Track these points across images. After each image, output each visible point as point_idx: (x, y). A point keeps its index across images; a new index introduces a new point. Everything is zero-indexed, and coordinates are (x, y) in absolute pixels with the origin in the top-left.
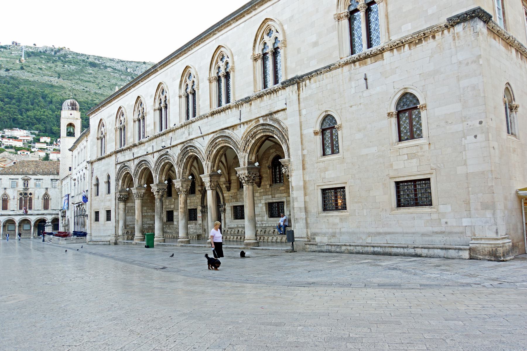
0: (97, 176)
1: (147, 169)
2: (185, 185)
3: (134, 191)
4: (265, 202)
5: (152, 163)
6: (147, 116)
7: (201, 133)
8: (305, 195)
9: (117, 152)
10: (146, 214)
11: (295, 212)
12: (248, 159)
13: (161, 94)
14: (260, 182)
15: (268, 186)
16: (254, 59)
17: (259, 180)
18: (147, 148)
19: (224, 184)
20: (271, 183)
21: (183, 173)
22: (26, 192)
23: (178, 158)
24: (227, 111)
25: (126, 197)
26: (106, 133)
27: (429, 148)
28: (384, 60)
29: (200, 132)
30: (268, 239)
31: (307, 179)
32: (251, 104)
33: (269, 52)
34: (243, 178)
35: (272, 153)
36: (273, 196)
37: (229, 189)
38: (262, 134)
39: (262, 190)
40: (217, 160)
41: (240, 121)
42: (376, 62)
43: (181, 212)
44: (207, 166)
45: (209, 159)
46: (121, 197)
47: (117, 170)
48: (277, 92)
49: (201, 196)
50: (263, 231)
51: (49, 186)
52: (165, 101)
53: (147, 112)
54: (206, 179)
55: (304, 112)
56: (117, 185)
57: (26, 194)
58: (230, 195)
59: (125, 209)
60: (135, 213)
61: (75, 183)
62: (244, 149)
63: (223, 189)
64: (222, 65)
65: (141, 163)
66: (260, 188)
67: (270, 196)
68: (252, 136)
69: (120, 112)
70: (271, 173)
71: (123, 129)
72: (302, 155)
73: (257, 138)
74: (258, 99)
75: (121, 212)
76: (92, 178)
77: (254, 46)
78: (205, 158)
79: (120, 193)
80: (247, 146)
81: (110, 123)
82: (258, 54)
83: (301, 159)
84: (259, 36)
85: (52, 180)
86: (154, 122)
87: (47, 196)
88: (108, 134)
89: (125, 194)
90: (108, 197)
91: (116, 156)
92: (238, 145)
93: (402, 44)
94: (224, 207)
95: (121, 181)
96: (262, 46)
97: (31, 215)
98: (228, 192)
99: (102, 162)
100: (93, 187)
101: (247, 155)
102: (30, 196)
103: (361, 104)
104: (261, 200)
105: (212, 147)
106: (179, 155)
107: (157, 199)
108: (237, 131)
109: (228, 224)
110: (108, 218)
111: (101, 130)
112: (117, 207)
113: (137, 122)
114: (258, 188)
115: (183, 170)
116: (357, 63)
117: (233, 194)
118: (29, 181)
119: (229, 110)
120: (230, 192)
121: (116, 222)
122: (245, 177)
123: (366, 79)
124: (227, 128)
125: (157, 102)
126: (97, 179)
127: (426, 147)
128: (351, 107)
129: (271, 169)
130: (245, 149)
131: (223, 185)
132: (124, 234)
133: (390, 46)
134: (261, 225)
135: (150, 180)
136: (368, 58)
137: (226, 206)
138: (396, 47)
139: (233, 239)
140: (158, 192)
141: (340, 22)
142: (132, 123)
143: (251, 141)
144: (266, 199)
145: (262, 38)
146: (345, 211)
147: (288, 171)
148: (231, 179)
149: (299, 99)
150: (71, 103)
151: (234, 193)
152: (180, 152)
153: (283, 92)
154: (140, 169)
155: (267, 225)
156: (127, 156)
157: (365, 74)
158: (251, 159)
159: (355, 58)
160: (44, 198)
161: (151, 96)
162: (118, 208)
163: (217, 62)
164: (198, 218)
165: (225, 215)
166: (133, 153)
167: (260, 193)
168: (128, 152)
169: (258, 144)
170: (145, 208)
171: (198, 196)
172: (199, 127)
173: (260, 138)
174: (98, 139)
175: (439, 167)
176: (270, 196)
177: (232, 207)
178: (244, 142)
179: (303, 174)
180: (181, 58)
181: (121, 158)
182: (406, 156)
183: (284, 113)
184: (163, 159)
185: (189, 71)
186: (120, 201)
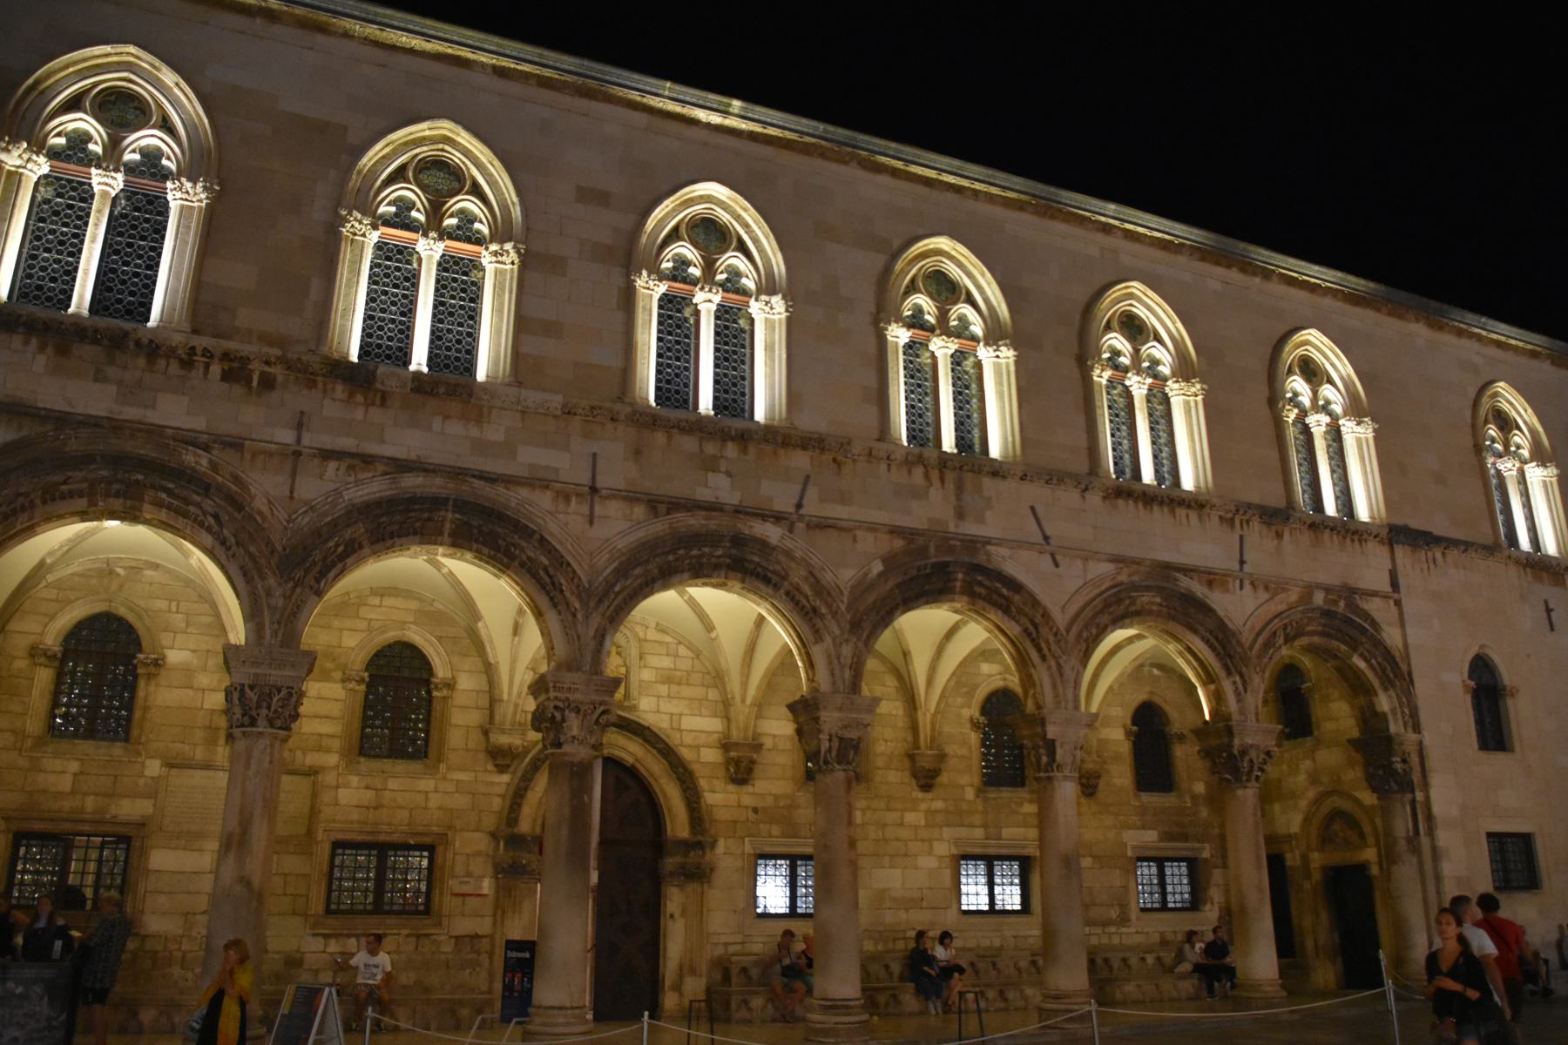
15: (970, 794)
39: (939, 805)
48: (1363, 543)
58: (747, 801)
66: (930, 795)
98: (731, 787)
104: (935, 844)
109: (723, 939)
114: (920, 795)
120: (749, 789)
151: (776, 797)
167: (929, 812)
172: (1033, 509)
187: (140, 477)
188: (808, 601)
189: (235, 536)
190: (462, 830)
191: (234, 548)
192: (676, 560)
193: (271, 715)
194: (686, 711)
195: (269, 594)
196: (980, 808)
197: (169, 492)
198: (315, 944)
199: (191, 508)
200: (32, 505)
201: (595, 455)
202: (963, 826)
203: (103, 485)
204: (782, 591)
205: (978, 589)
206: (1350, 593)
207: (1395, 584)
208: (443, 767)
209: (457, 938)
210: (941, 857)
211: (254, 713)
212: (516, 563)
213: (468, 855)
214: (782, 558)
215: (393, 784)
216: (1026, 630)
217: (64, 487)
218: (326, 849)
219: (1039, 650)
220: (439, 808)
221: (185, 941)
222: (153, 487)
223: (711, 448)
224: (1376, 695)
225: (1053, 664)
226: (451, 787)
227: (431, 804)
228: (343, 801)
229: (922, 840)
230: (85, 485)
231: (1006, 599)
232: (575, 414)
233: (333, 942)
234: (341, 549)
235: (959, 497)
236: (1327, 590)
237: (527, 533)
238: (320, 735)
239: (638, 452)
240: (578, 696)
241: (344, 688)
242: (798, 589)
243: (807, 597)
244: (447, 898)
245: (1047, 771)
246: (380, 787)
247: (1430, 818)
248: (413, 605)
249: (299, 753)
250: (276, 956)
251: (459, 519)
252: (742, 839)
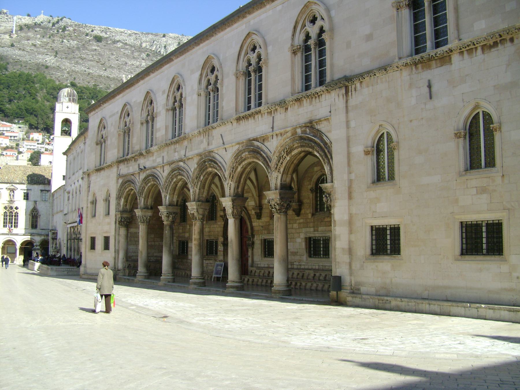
0: (94, 192)
1: (155, 186)
2: (201, 211)
3: (138, 212)
4: (305, 236)
5: (162, 179)
6: (158, 118)
7: (224, 143)
8: (351, 232)
9: (120, 162)
10: (153, 243)
11: (337, 254)
12: (281, 181)
13: (176, 90)
14: (300, 210)
15: (310, 216)
16: (293, 52)
17: (298, 207)
18: (156, 159)
19: (253, 209)
20: (314, 212)
21: (199, 194)
22: (11, 205)
23: (193, 173)
24: (256, 116)
25: (128, 221)
26: (107, 137)
27: (503, 181)
28: (451, 64)
29: (222, 142)
30: (305, 286)
31: (354, 211)
32: (287, 109)
33: (312, 45)
34: (274, 205)
35: (317, 171)
36: (316, 228)
37: (259, 216)
38: (300, 149)
39: (302, 221)
40: (242, 180)
41: (273, 131)
42: (442, 66)
43: (195, 244)
44: (229, 187)
45: (232, 178)
46: (123, 220)
47: (119, 185)
48: (320, 96)
49: (223, 223)
50: (301, 274)
51: (38, 199)
52: (181, 100)
53: (158, 111)
54: (227, 203)
55: (353, 124)
56: (118, 204)
57: (11, 208)
58: (261, 224)
59: (127, 236)
60: (138, 241)
61: (69, 197)
62: (276, 168)
63: (251, 216)
64: (253, 57)
65: (148, 179)
66: (299, 218)
67: (312, 229)
68: (286, 151)
69: (125, 112)
70: (314, 198)
71: (127, 132)
72: (348, 179)
73: (293, 153)
74: (296, 104)
75: (122, 240)
76: (88, 194)
77: (293, 35)
78: (226, 176)
79: (121, 215)
80: (280, 164)
81: (112, 124)
82: (297, 46)
83: (347, 185)
84: (300, 23)
85: (42, 191)
86: (166, 126)
87: (36, 212)
88: (109, 138)
89: (127, 217)
90: (107, 220)
91: (118, 167)
92: (269, 162)
93: (474, 47)
94: (253, 240)
95: (123, 200)
96: (302, 37)
97: (17, 235)
98: (258, 221)
99: (101, 173)
100: (89, 205)
101: (280, 176)
102: (16, 211)
103: (422, 119)
105: (237, 162)
106: (195, 169)
107: (166, 225)
108: (269, 143)
110: (107, 247)
111: (101, 133)
112: (117, 232)
113: (145, 125)
114: (297, 218)
115: (199, 190)
116: (419, 66)
117: (265, 223)
118: (15, 191)
119: (260, 116)
120: (261, 220)
121: (115, 252)
122: (276, 204)
123: (430, 86)
124: (256, 140)
125: (171, 101)
126: (94, 194)
127: (499, 180)
128: (411, 121)
129: (314, 193)
130: (278, 167)
131: (251, 210)
132: (125, 267)
133: (459, 48)
134: (299, 267)
135: (158, 200)
136: (432, 60)
137: (255, 238)
138: (466, 49)
139: (262, 282)
140: (168, 217)
141: (400, 12)
142: (139, 125)
143: (285, 157)
145: (304, 26)
146: (399, 256)
147: (331, 200)
148: (263, 203)
149: (347, 107)
150: (68, 93)
151: (266, 222)
152: (196, 166)
153: (327, 96)
154: (147, 185)
155: (306, 267)
156: (131, 168)
157: (429, 81)
158: (285, 181)
159: (417, 60)
160: (32, 214)
161: (164, 92)
162: (119, 235)
163: (247, 53)
165: (252, 250)
166: (139, 165)
168: (132, 163)
169: (295, 162)
170: (153, 236)
171: (219, 223)
172: (221, 135)
173: (297, 154)
174: (97, 144)
175: (512, 206)
176: (312, 229)
177: (262, 241)
178: (276, 158)
179: (349, 206)
180: (201, 45)
181: (125, 169)
182: (475, 190)
183: (328, 123)
184: (175, 174)
185: (212, 62)
186: (122, 225)
196: (312, 221)
202: (308, 227)
218: (206, 241)
229: (298, 233)
233: (206, 261)
236: (301, 127)
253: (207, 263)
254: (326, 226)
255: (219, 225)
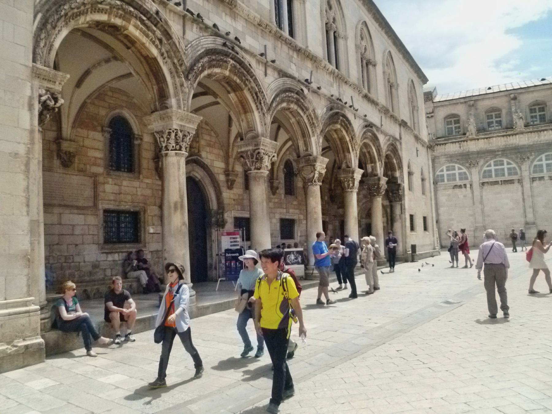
15: (283, 196)
39: (276, 200)
58: (232, 196)
66: (275, 197)
98: (228, 191)
104: (276, 214)
117: (237, 196)
120: (232, 192)
144: (281, 213)
151: (239, 195)
164: (148, 238)
167: (274, 203)
172: (351, 97)
176: (285, 211)
187: (132, 9)
188: (312, 120)
189: (167, 52)
190: (149, 205)
191: (167, 59)
192: (286, 97)
193: (187, 146)
194: (215, 159)
195: (182, 85)
197: (142, 21)
198: (103, 257)
199: (150, 33)
200: (87, 13)
201: (265, 46)
203: (115, 10)
204: (306, 115)
205: (343, 124)
206: (395, 139)
207: (401, 138)
208: (141, 176)
209: (152, 252)
210: (277, 219)
211: (181, 143)
212: (247, 88)
213: (152, 216)
214: (307, 102)
215: (125, 183)
216: (350, 140)
217: (100, 6)
219: (352, 147)
220: (141, 195)
221: (51, 258)
222: (136, 17)
223: (291, 53)
224: (396, 171)
225: (355, 152)
226: (144, 186)
227: (139, 193)
228: (107, 190)
230: (108, 7)
231: (348, 128)
232: (261, 26)
233: (109, 256)
234: (200, 69)
235: (339, 90)
237: (252, 76)
238: (96, 158)
239: (275, 49)
240: (266, 149)
241: (103, 135)
242: (310, 115)
243: (312, 119)
244: (147, 235)
245: (351, 189)
246: (120, 184)
247: (405, 209)
248: (124, 98)
249: (88, 167)
250: (89, 263)
251: (233, 64)
252: (231, 211)
253: (114, 261)
254: (295, 209)
255: (147, 183)
